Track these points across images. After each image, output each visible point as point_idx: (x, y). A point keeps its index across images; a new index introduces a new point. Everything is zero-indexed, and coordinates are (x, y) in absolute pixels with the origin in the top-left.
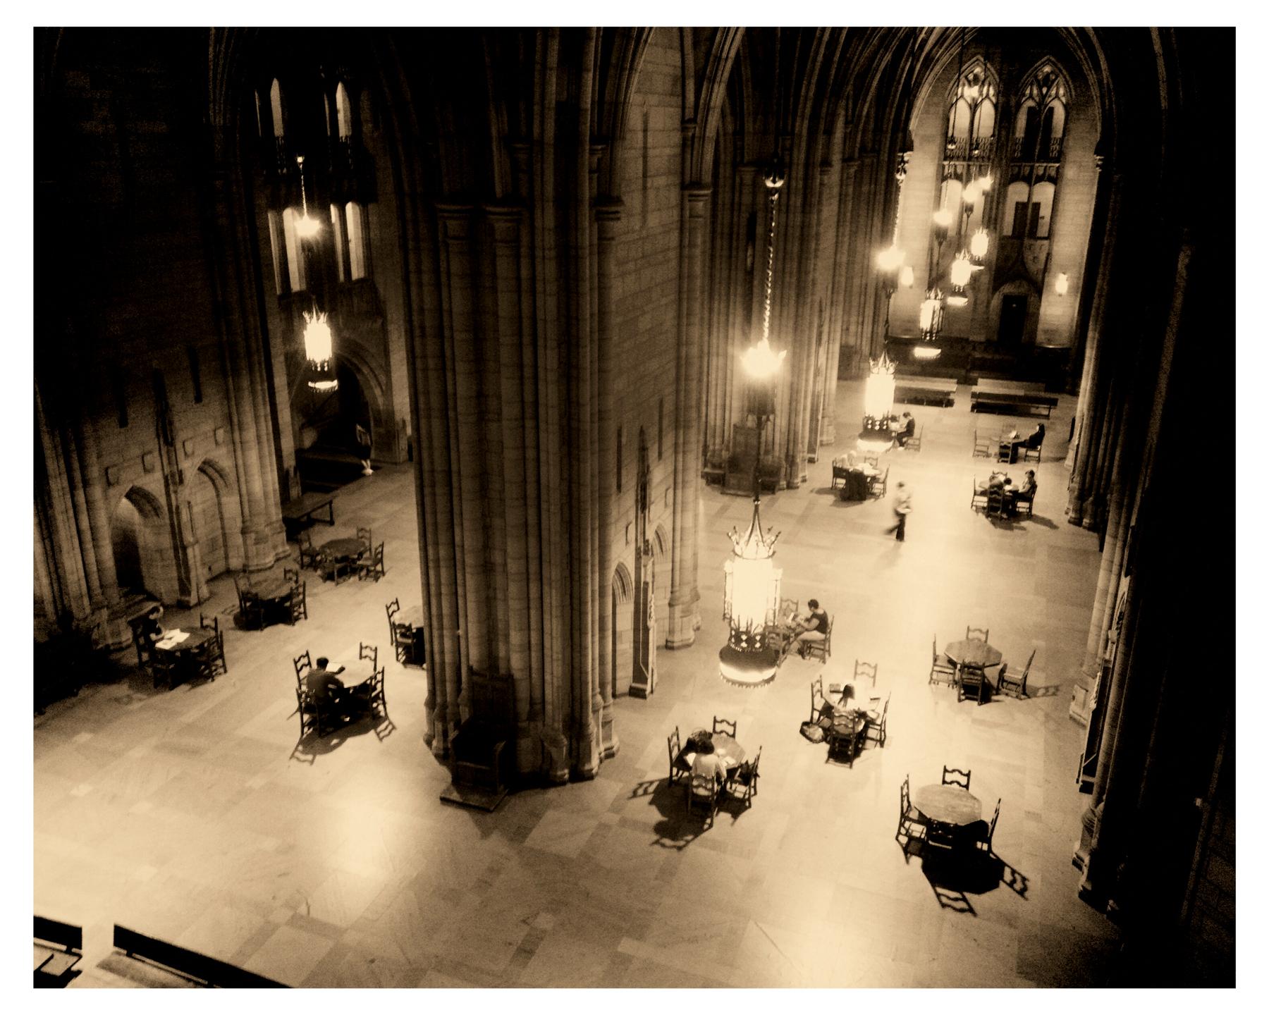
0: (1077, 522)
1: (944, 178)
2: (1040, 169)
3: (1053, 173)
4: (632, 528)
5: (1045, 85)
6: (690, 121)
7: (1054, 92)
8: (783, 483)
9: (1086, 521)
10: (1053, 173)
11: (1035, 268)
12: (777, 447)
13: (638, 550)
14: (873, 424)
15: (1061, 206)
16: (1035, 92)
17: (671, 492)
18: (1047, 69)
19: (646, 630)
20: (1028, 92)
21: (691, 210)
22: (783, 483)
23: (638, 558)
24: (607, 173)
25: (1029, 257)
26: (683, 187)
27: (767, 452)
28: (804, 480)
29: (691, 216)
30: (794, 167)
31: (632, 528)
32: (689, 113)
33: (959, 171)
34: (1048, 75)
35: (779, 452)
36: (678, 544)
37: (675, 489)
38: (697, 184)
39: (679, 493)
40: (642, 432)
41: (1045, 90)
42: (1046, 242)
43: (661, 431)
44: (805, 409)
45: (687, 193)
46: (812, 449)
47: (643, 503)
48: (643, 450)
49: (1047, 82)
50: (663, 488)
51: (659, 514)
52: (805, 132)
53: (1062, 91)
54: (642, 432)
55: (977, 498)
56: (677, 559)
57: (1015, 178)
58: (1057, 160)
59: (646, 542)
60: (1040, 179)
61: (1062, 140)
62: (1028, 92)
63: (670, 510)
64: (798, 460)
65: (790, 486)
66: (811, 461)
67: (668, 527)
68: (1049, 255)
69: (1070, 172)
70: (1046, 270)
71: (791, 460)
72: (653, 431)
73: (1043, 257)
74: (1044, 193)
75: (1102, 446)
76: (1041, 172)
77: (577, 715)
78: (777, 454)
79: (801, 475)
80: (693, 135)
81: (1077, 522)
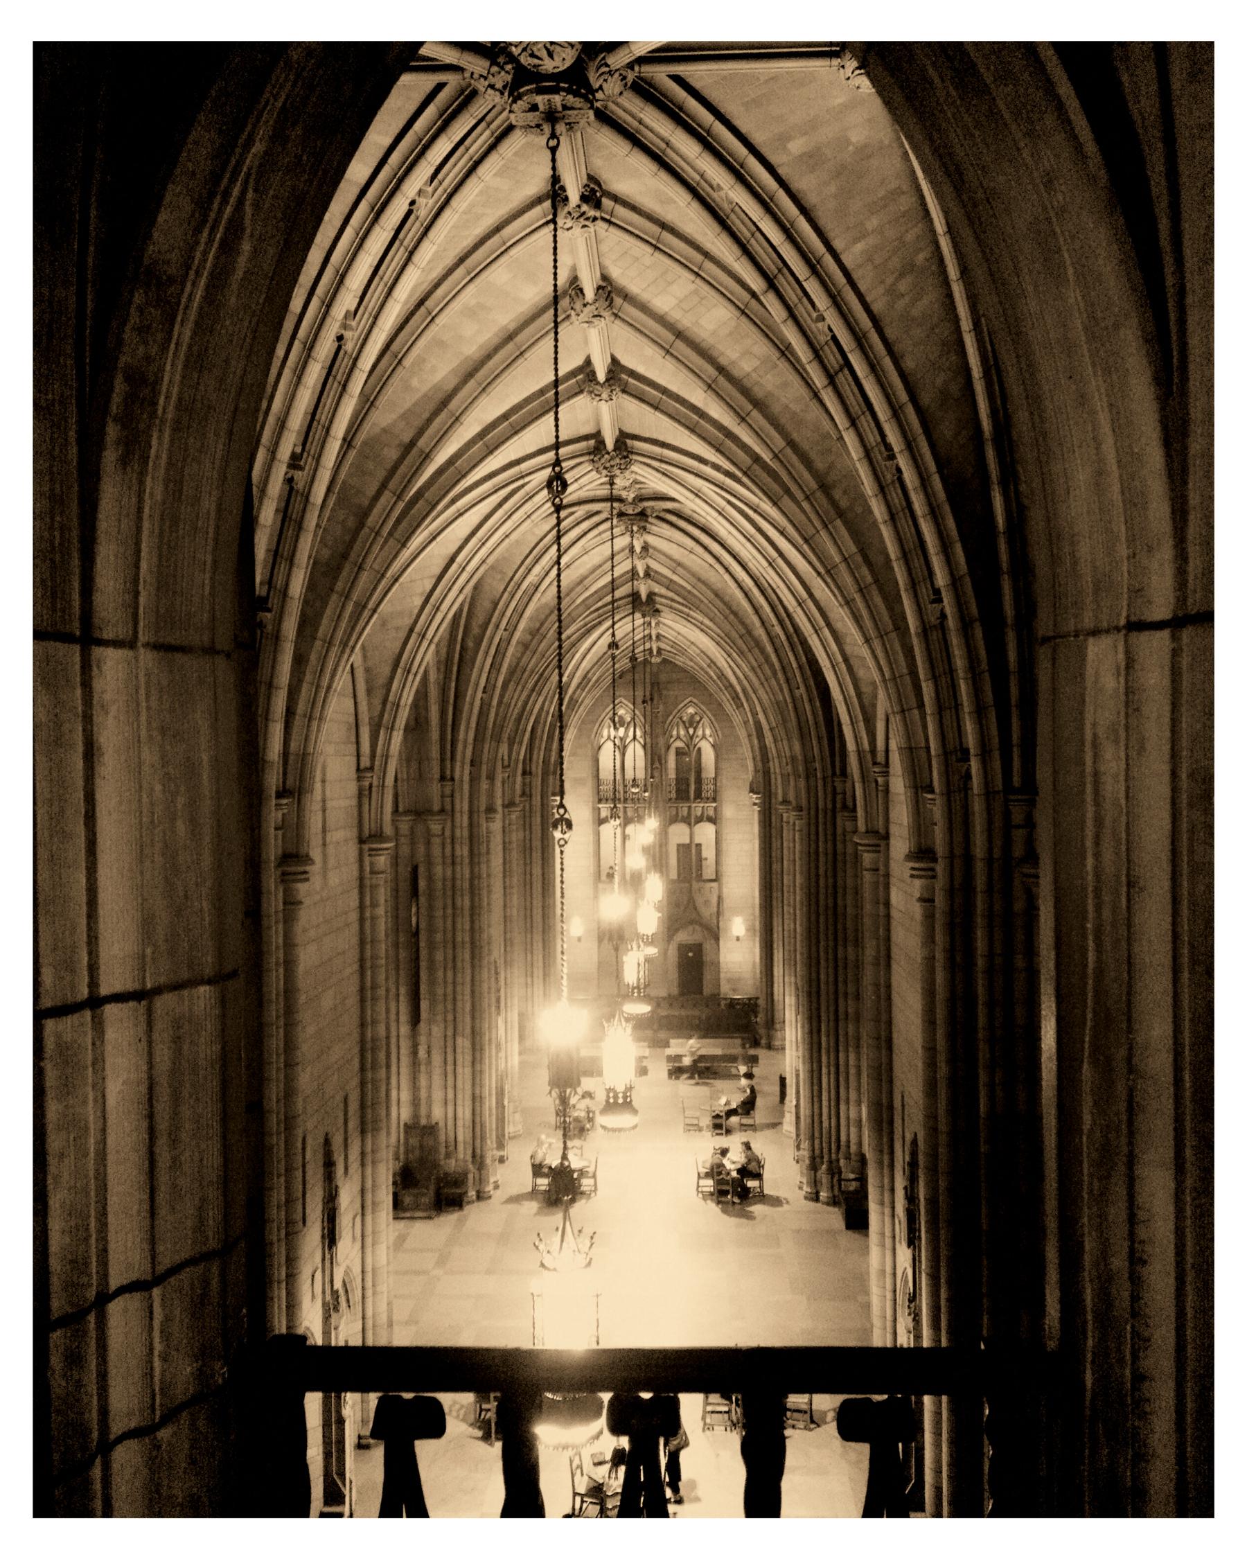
0: (815, 1197)
1: (601, 822)
2: (698, 808)
3: (711, 813)
4: (318, 1275)
5: (691, 725)
6: (367, 769)
7: (700, 732)
9: (823, 1195)
11: (707, 912)
12: (461, 1147)
13: (325, 1304)
14: (616, 1097)
15: (724, 846)
16: (682, 732)
17: (358, 1219)
18: (691, 710)
19: (341, 1421)
20: (675, 733)
21: (372, 864)
22: (472, 1193)
23: (327, 1318)
24: (294, 828)
25: (699, 901)
26: (361, 841)
27: (448, 1156)
28: (496, 1187)
29: (372, 872)
30: (458, 815)
31: (318, 1275)
32: (365, 762)
34: (692, 716)
35: (463, 1153)
36: (369, 1293)
37: (363, 1215)
38: (378, 836)
39: (369, 1218)
40: (327, 1142)
41: (691, 731)
42: (714, 885)
43: (346, 1140)
44: (490, 1095)
45: (366, 847)
46: (501, 1146)
47: (330, 1238)
48: (329, 1164)
49: (692, 723)
50: (351, 1216)
51: (347, 1248)
52: (466, 778)
53: (708, 732)
54: (327, 1142)
55: (702, 1182)
56: (369, 1313)
57: (674, 820)
58: (714, 800)
59: (335, 1294)
60: (699, 820)
61: (715, 779)
62: (675, 733)
63: (359, 1244)
64: (488, 1161)
65: (480, 1197)
66: (502, 1160)
67: (357, 1270)
69: (728, 811)
71: (478, 1160)
72: (337, 1141)
73: (714, 900)
74: (705, 833)
75: (825, 1103)
76: (699, 814)
78: (461, 1156)
79: (492, 1180)
80: (371, 786)
81: (815, 1197)
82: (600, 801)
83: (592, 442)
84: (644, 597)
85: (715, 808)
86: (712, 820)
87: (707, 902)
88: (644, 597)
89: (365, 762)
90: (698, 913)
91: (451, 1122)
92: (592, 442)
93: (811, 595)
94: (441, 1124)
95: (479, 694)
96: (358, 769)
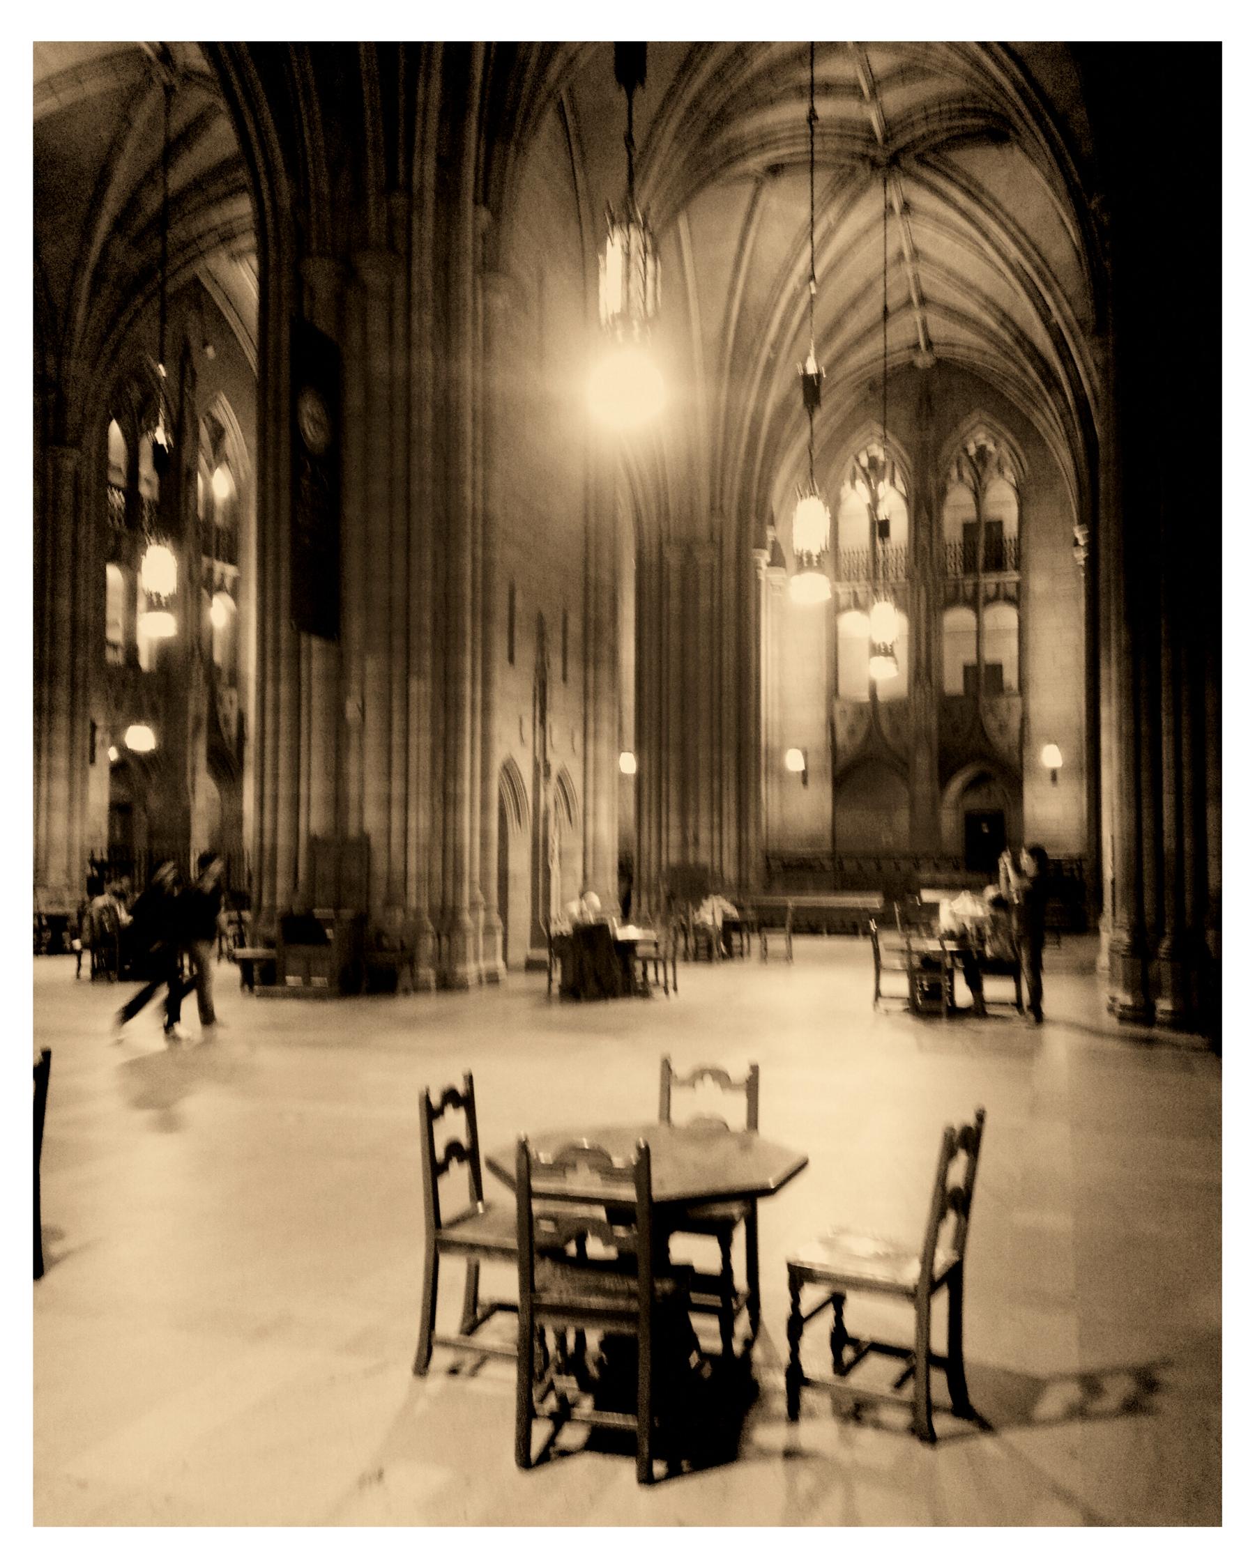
2: (989, 581)
3: (1012, 590)
8: (427, 973)
9: (1164, 1005)
10: (1012, 590)
11: (1004, 743)
15: (1031, 638)
22: (427, 973)
25: (991, 724)
27: (389, 903)
35: (416, 898)
57: (952, 601)
60: (991, 600)
65: (448, 983)
68: (1024, 720)
69: (1039, 584)
71: (448, 920)
73: (1015, 723)
75: (1168, 800)
78: (412, 902)
85: (1018, 585)
87: (1003, 728)
91: (396, 840)
94: (377, 841)
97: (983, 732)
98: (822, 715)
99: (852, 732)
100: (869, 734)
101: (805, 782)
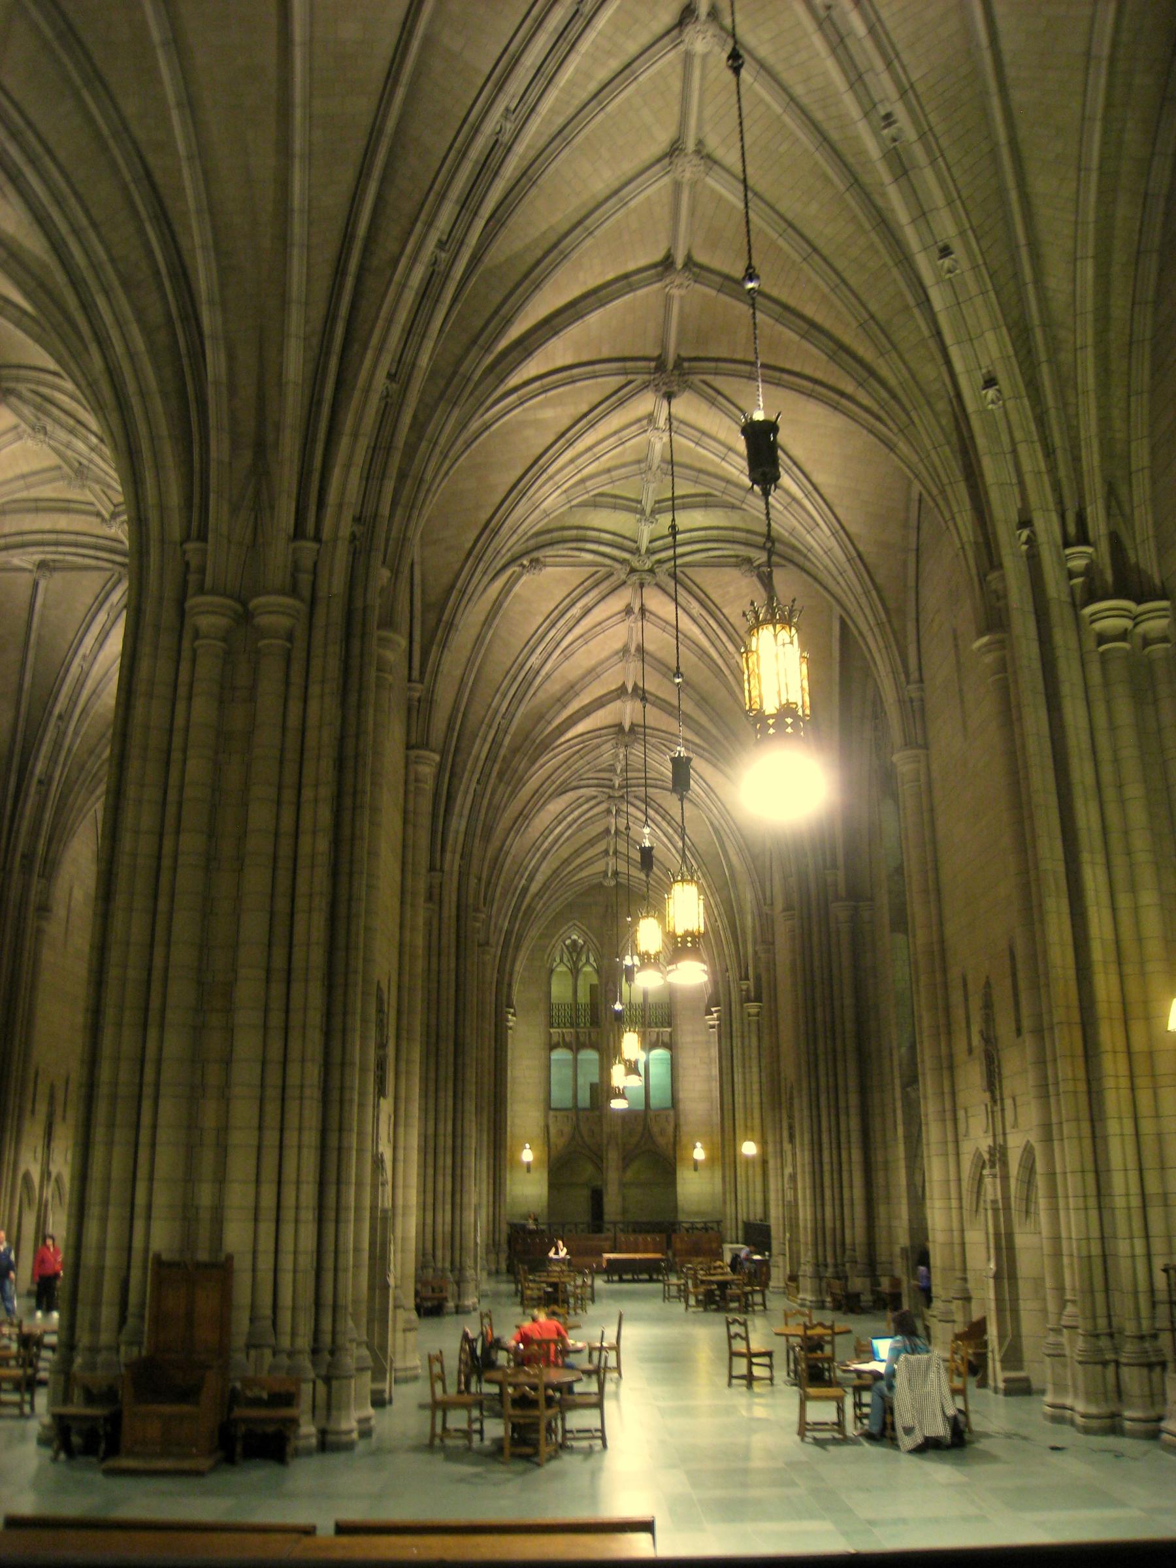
1: (552, 1047)
3: (666, 1039)
10: (666, 1039)
22: (451, 1304)
25: (655, 1130)
26: (409, 747)
32: (416, 674)
33: (567, 1039)
45: (413, 753)
52: (456, 868)
58: (670, 1025)
68: (677, 1127)
70: (676, 1143)
73: (671, 1129)
77: (327, 1338)
82: (552, 1026)
83: (653, 364)
84: (627, 728)
86: (670, 1046)
87: (663, 1132)
88: (627, 728)
89: (416, 674)
90: (654, 1143)
92: (653, 364)
93: (843, 528)
95: (474, 785)
96: (410, 680)
97: (651, 1136)
98: (542, 1123)
99: (561, 1133)
100: (573, 1138)
101: (529, 1170)
